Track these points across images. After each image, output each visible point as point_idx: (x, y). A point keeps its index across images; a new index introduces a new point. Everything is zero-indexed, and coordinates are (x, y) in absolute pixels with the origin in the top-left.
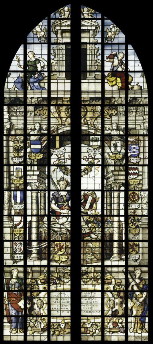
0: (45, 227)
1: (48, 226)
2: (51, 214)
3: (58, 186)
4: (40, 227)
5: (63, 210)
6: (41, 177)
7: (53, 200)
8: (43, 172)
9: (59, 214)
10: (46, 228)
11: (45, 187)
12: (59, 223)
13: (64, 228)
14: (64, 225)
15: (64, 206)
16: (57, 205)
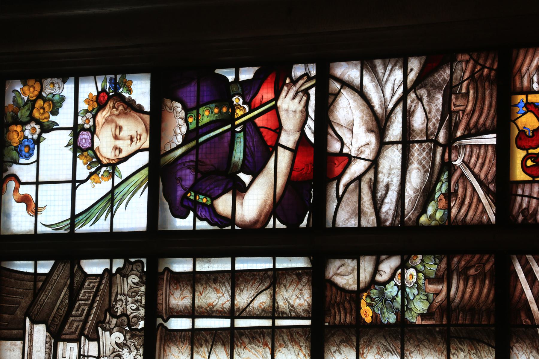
0: (397, 280)
1: (390, 254)
2: (304, 224)
3: (125, 169)
4: (401, 313)
5: (278, 129)
6: (68, 314)
7: (212, 208)
8: (37, 293)
9: (307, 158)
10: (403, 266)
11: (133, 279)
12: (369, 153)
13: (407, 115)
14: (388, 116)
15: (259, 122)
16: (246, 178)
